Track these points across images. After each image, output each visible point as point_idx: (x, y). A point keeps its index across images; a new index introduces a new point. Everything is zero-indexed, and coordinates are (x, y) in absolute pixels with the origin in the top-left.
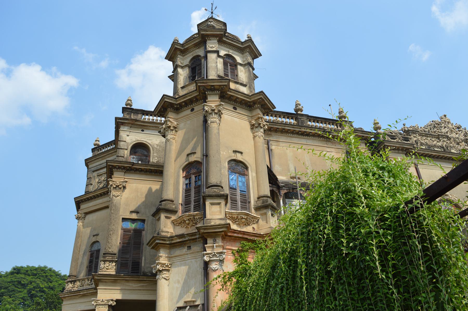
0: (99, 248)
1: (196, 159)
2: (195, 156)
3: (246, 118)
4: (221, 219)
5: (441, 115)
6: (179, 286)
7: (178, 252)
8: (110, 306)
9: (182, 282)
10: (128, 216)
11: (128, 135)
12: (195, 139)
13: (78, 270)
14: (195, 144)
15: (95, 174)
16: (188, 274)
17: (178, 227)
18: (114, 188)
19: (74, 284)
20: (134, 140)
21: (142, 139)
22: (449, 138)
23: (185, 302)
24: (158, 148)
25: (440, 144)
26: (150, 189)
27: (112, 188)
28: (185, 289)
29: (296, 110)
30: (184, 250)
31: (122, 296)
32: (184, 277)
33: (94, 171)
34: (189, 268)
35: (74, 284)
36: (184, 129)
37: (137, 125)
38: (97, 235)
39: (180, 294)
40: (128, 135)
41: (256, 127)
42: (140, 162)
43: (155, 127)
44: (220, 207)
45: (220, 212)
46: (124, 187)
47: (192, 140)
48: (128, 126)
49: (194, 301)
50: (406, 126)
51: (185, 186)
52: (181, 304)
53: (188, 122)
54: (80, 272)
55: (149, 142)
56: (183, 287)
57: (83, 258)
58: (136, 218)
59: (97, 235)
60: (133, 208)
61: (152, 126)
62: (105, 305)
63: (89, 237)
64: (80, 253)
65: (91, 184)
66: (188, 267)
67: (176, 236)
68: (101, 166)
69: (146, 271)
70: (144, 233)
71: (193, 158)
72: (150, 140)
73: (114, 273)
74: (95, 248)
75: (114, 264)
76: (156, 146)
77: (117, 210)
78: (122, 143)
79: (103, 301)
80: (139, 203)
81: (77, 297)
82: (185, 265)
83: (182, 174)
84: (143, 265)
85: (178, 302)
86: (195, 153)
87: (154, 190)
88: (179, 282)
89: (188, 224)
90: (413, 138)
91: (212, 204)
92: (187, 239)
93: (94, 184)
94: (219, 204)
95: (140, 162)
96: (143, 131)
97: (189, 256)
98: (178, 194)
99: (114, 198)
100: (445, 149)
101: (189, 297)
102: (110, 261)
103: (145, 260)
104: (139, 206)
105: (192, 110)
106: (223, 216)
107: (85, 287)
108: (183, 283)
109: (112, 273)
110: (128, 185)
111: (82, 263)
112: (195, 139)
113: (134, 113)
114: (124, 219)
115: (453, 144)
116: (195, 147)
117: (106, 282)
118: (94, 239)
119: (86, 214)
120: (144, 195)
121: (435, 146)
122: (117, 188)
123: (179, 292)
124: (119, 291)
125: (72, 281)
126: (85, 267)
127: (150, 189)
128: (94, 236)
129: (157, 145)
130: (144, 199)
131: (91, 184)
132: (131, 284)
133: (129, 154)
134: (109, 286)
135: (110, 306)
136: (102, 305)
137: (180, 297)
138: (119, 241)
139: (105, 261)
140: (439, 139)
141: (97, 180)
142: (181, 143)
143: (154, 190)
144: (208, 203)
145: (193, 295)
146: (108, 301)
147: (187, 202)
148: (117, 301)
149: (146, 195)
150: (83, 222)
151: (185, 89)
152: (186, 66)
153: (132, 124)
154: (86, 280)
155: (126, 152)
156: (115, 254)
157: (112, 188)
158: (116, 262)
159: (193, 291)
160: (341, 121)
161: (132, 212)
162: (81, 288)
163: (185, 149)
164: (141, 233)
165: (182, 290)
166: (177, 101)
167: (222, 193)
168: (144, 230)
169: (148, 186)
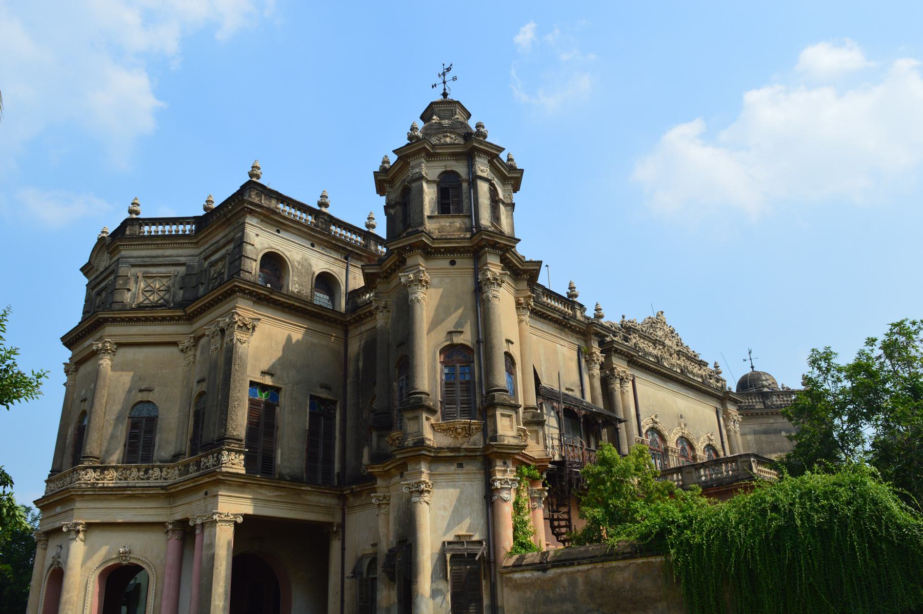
0: (153, 414)
1: (463, 342)
2: (462, 336)
3: (512, 290)
4: (514, 437)
5: (657, 310)
6: (447, 514)
7: (442, 469)
8: (236, 523)
9: (450, 510)
10: (259, 379)
11: (257, 235)
12: (460, 311)
13: (104, 449)
14: (460, 318)
15: (139, 271)
16: (459, 500)
17: (439, 434)
18: (239, 326)
19: (102, 473)
20: (266, 245)
21: (278, 247)
22: (664, 345)
23: (459, 536)
24: (300, 267)
25: (655, 352)
26: (289, 338)
27: (236, 326)
28: (456, 517)
29: (570, 296)
30: (453, 468)
31: (254, 510)
32: (454, 504)
33: (133, 266)
34: (461, 493)
35: (102, 473)
36: (439, 287)
37: (273, 219)
38: (149, 390)
39: (448, 525)
40: (257, 235)
41: (524, 308)
42: (269, 285)
43: (299, 230)
44: (511, 421)
45: (512, 427)
46: (254, 327)
47: (456, 310)
48: (257, 218)
49: (471, 536)
50: (626, 319)
51: (444, 377)
52: (450, 537)
53: (447, 280)
54: (108, 452)
55: (288, 254)
56: (453, 517)
57: (116, 426)
58: (270, 383)
59: (149, 390)
60: (265, 367)
61: (294, 228)
62: (230, 521)
63: (130, 391)
64: (107, 417)
65: (129, 290)
66: (459, 490)
67: (448, 448)
68: (154, 260)
69: (284, 472)
70: (278, 409)
71: (458, 340)
72: (289, 251)
73: (244, 472)
74: (145, 412)
75: (242, 457)
76: (296, 264)
77: (244, 366)
78: (249, 247)
79: (227, 516)
80: (274, 360)
81: (113, 498)
82: (454, 487)
83: (439, 358)
84: (279, 461)
85: (445, 534)
86: (461, 332)
87: (294, 340)
88: (445, 509)
89: (459, 434)
90: (634, 339)
91: (502, 415)
92: (462, 454)
93: (133, 290)
94: (510, 416)
95: (269, 285)
96: (278, 231)
97: (461, 477)
98: (436, 386)
99: (239, 343)
100: (659, 360)
101: (462, 530)
102: (237, 452)
103: (282, 454)
104: (273, 366)
105: (453, 263)
106: (514, 433)
107: (131, 483)
108: (453, 512)
109: (240, 472)
110: (260, 327)
111: (113, 436)
112: (460, 311)
113: (266, 195)
114: (253, 384)
115: (667, 356)
116: (460, 323)
117: (230, 485)
118: (140, 397)
119: (120, 345)
120: (281, 347)
121: (650, 354)
122: (244, 328)
123: (446, 523)
124: (249, 501)
125: (98, 467)
126: (122, 444)
127: (289, 338)
128: (141, 391)
129: (299, 263)
130: (280, 354)
131: (129, 290)
132: (264, 492)
133: (258, 270)
134: (235, 491)
135: (236, 523)
136: (226, 521)
137: (449, 528)
138: (246, 421)
139: (229, 450)
140: (654, 344)
141: (142, 285)
142: (436, 310)
143: (294, 340)
144: (498, 412)
145: (470, 526)
146: (236, 515)
147: (448, 399)
148: (246, 516)
149: (284, 347)
150: (111, 360)
151: (434, 220)
152: (434, 182)
153: (265, 216)
154: (135, 471)
155: (254, 264)
156: (241, 440)
157: (236, 326)
158: (244, 453)
159: (467, 522)
160: (570, 301)
161: (264, 373)
162: (123, 483)
163: (443, 320)
164: (275, 409)
165: (450, 520)
166: (433, 243)
167: (513, 402)
168: (278, 405)
169: (287, 333)
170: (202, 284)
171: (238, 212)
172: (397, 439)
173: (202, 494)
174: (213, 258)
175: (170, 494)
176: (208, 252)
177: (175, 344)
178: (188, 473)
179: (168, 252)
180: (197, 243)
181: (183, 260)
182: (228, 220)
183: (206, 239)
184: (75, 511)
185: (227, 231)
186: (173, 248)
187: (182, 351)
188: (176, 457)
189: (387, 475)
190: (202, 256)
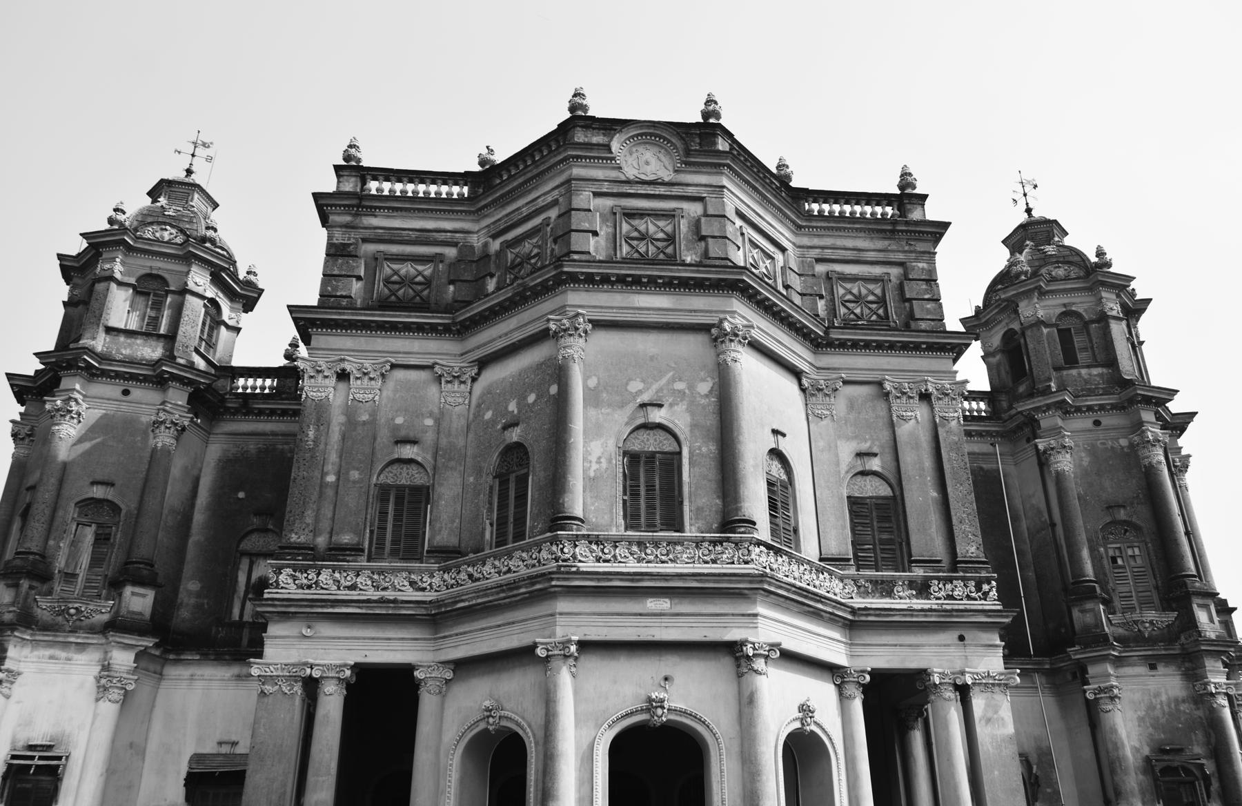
170: (821, 297)
171: (923, 232)
172: (1151, 622)
173: (955, 634)
174: (838, 268)
175: (855, 624)
176: (828, 254)
177: (796, 373)
178: (889, 594)
179: (769, 218)
180: (799, 227)
181: (785, 243)
182: (893, 231)
183: (823, 232)
184: (760, 620)
185: (880, 244)
186: (774, 216)
187: (803, 390)
188: (829, 561)
189: (1119, 662)
190: (815, 253)
